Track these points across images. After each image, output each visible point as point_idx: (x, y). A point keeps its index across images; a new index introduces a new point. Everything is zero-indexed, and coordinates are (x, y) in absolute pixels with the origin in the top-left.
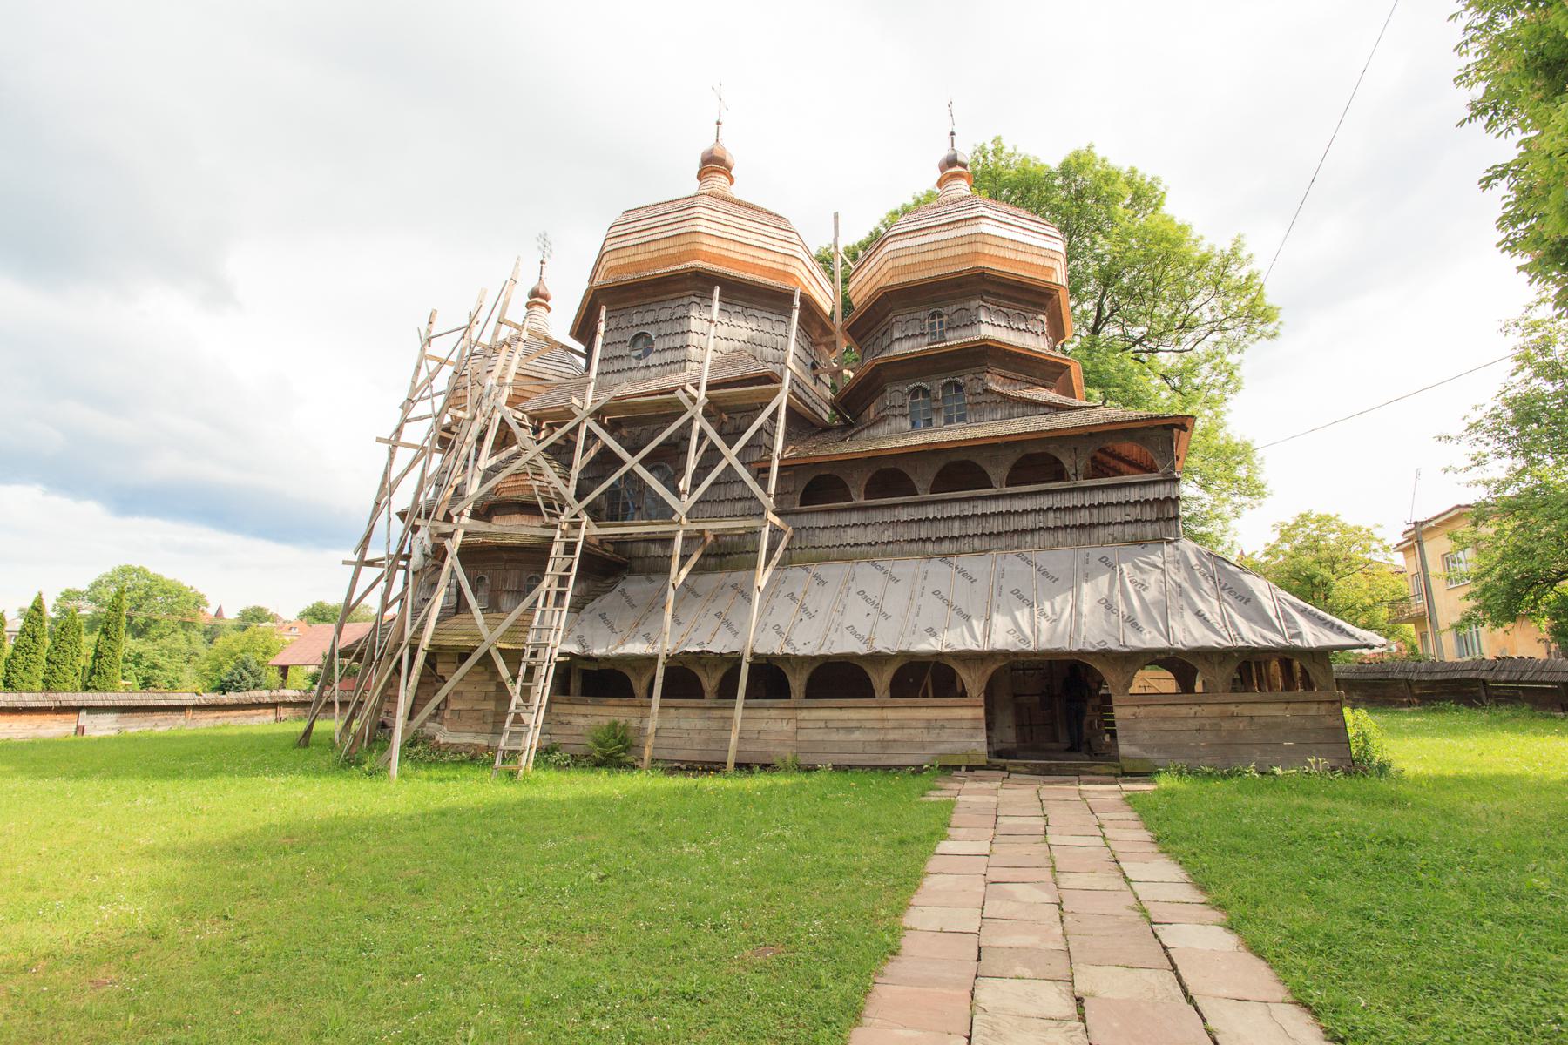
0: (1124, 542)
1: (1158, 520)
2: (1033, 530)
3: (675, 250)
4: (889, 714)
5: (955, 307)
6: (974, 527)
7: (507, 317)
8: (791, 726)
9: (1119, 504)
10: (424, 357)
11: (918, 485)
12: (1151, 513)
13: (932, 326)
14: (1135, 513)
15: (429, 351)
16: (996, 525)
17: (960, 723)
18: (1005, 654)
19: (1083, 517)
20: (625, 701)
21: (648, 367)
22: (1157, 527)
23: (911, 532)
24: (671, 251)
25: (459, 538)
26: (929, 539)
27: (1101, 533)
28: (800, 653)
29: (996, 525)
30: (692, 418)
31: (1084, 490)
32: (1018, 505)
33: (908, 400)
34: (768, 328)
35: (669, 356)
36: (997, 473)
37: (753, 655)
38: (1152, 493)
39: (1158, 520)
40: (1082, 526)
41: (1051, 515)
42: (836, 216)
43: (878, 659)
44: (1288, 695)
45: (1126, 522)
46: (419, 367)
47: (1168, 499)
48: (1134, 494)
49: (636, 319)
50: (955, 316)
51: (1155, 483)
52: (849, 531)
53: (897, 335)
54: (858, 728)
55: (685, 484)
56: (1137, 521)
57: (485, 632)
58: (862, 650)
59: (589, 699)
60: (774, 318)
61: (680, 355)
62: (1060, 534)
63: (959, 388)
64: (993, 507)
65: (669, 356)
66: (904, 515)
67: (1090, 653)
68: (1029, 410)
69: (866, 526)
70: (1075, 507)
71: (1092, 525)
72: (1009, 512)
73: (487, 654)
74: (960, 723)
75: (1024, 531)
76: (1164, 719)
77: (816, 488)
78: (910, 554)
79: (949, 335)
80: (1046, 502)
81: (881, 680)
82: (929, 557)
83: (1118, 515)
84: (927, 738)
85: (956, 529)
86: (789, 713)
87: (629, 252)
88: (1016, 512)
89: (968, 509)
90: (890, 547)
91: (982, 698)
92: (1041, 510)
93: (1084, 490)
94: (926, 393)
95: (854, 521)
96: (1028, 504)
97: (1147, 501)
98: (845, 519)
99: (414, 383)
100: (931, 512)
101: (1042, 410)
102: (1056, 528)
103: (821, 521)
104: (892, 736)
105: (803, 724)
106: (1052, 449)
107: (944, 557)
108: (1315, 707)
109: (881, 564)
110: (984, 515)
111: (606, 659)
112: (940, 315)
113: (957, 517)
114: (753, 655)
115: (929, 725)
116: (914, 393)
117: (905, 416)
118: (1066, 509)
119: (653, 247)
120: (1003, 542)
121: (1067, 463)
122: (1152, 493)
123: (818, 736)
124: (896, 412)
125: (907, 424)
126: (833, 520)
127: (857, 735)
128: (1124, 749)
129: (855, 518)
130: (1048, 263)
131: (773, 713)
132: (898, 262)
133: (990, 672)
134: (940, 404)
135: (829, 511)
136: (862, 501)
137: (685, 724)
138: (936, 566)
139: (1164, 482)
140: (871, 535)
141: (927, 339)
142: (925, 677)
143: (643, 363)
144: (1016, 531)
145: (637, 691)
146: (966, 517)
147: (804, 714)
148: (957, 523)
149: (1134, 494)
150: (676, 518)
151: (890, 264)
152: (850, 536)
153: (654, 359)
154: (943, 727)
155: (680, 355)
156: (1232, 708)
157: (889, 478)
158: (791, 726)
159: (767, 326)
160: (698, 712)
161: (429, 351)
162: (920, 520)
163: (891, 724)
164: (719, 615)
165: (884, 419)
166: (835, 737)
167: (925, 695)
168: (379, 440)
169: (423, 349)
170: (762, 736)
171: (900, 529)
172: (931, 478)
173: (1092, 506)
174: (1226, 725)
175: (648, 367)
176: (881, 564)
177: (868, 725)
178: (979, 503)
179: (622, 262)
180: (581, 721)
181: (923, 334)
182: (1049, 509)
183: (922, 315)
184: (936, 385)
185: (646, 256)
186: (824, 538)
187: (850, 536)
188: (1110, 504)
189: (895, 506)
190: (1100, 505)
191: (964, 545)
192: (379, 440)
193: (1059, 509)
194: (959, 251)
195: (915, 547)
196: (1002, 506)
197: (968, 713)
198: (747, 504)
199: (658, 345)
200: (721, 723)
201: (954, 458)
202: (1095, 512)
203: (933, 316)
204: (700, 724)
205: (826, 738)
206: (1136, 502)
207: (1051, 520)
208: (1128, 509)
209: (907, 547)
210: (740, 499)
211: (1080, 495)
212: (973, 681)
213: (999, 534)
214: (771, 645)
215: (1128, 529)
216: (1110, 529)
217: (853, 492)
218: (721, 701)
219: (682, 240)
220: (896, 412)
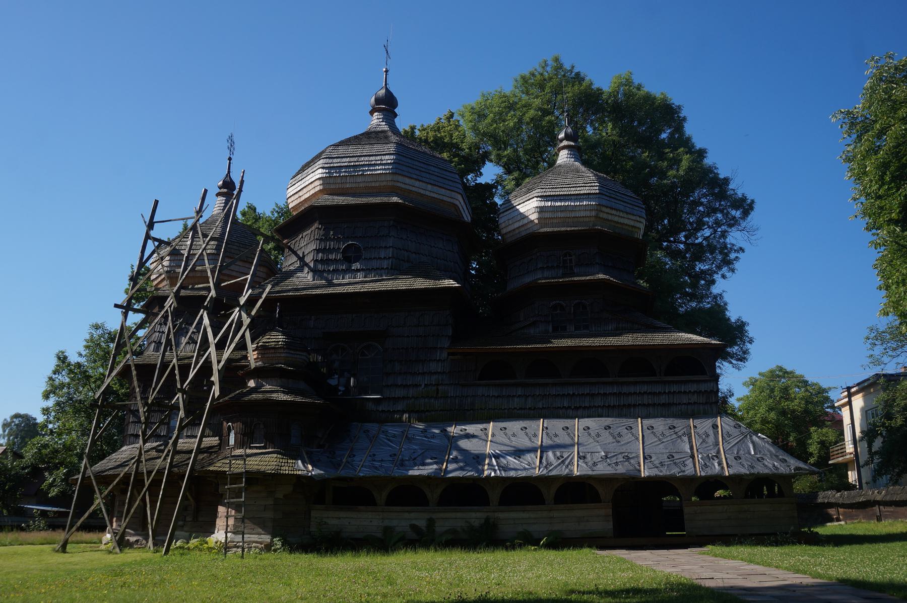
2: (635, 406)
9: (685, 392)
10: (148, 237)
14: (694, 398)
15: (153, 233)
19: (663, 399)
26: (569, 407)
38: (703, 387)
45: (689, 404)
47: (712, 391)
56: (695, 403)
64: (609, 390)
70: (660, 393)
72: (620, 393)
80: (645, 388)
96: (632, 389)
97: (700, 391)
102: (649, 405)
110: (605, 394)
112: (570, 256)
118: (654, 394)
122: (703, 387)
129: (520, 392)
130: (638, 225)
139: (710, 381)
149: (693, 387)
161: (153, 233)
162: (564, 395)
168: (116, 306)
188: (680, 392)
192: (116, 306)
193: (650, 393)
206: (695, 392)
207: (646, 400)
213: (614, 406)
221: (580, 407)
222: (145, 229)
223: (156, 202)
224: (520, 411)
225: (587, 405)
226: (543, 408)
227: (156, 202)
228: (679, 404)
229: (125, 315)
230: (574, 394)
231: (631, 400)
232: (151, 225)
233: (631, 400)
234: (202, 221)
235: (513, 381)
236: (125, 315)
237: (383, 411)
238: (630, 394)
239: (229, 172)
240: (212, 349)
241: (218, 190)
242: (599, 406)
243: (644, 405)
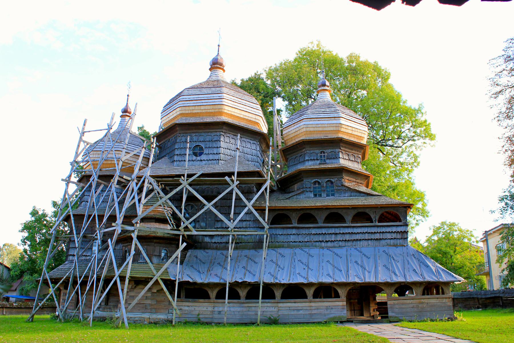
0: (390, 245)
1: (401, 238)
2: (360, 240)
3: (213, 111)
4: (313, 304)
5: (330, 151)
6: (339, 238)
8: (276, 309)
9: (389, 232)
10: (81, 140)
11: (319, 221)
12: (399, 236)
13: (321, 156)
14: (394, 236)
16: (347, 237)
17: (338, 306)
18: (355, 284)
19: (377, 236)
20: (207, 300)
21: (201, 160)
22: (401, 241)
23: (316, 238)
24: (211, 111)
25: (136, 233)
26: (323, 241)
27: (383, 242)
28: (282, 282)
29: (347, 237)
30: (232, 190)
31: (378, 226)
32: (356, 230)
33: (312, 186)
34: (249, 147)
35: (211, 157)
36: (349, 218)
37: (264, 283)
38: (400, 229)
39: (401, 238)
40: (377, 239)
41: (367, 235)
43: (310, 285)
44: (438, 296)
46: (79, 146)
47: (405, 231)
48: (394, 229)
49: (195, 139)
50: (330, 154)
51: (401, 226)
52: (291, 236)
53: (307, 158)
54: (301, 310)
55: (232, 216)
56: (395, 238)
57: (155, 272)
58: (305, 281)
59: (190, 300)
60: (252, 142)
61: (216, 157)
62: (370, 241)
63: (332, 183)
65: (211, 157)
66: (314, 231)
67: (381, 283)
68: (358, 194)
69: (298, 235)
70: (375, 233)
71: (380, 239)
72: (352, 233)
73: (157, 282)
75: (357, 240)
76: (403, 304)
77: (280, 218)
78: (316, 246)
79: (328, 161)
80: (365, 230)
81: (310, 292)
82: (323, 248)
83: (389, 236)
84: (326, 312)
85: (333, 238)
86: (275, 305)
87: (191, 108)
88: (355, 233)
89: (337, 231)
90: (308, 243)
91: (345, 298)
92: (363, 233)
93: (378, 226)
94: (319, 183)
97: (398, 232)
98: (290, 231)
99: (77, 153)
100: (324, 231)
101: (362, 195)
102: (368, 239)
103: (280, 232)
104: (314, 312)
105: (280, 309)
106: (367, 211)
107: (328, 248)
108: (445, 299)
109: (305, 250)
110: (343, 233)
111: (202, 284)
112: (324, 153)
113: (333, 233)
114: (264, 283)
115: (327, 308)
116: (315, 183)
117: (311, 192)
118: (372, 233)
119: (202, 108)
120: (350, 243)
121: (372, 216)
122: (400, 229)
123: (286, 313)
124: (308, 190)
125: (312, 195)
126: (285, 232)
127: (301, 312)
128: (390, 314)
129: (294, 231)
130: (363, 136)
131: (269, 305)
132: (308, 129)
133: (348, 289)
134: (324, 189)
135: (283, 228)
136: (296, 225)
137: (232, 309)
138: (326, 252)
139: (404, 225)
140: (300, 238)
141: (318, 162)
142: (325, 291)
143: (199, 158)
144: (354, 240)
145: (211, 296)
146: (336, 234)
148: (333, 236)
149: (394, 229)
150: (229, 229)
151: (304, 130)
152: (292, 238)
153: (203, 157)
154: (332, 308)
155: (216, 157)
156: (422, 300)
158: (276, 309)
159: (249, 145)
160: (238, 305)
161: (84, 138)
162: (320, 234)
163: (313, 308)
164: (244, 267)
165: (303, 192)
166: (292, 313)
167: (321, 298)
168: (63, 180)
169: (81, 138)
170: (265, 313)
171: (312, 237)
172: (324, 218)
173: (380, 232)
174: (420, 306)
175: (201, 160)
176: (305, 250)
177: (305, 308)
178: (342, 229)
179: (187, 112)
180: (187, 308)
181: (317, 159)
182: (366, 232)
183: (317, 151)
184: (323, 180)
185: (199, 111)
186: (281, 239)
187: (292, 238)
188: (387, 232)
189: (310, 228)
190: (383, 232)
191: (335, 244)
192: (63, 180)
193: (369, 233)
194: (332, 129)
195: (317, 244)
196: (350, 230)
197: (341, 304)
198: (248, 223)
199: (206, 151)
200: (248, 309)
201: (333, 211)
202: (381, 234)
203: (321, 153)
204: (239, 309)
205: (289, 313)
206: (395, 232)
207: (367, 236)
208: (392, 234)
209: (314, 243)
210: (245, 221)
211: (377, 228)
212: (343, 292)
213: (348, 240)
214: (269, 280)
215: (392, 241)
216: (386, 241)
217: (293, 221)
218: (248, 301)
219: (216, 107)
220: (308, 190)
222: (80, 135)
223: (85, 121)
224: (294, 243)
227: (85, 121)
229: (67, 185)
231: (358, 237)
232: (83, 133)
233: (358, 237)
234: (112, 131)
235: (290, 226)
236: (67, 185)
237: (215, 243)
238: (358, 233)
239: (127, 104)
240: (116, 205)
241: (121, 114)
242: (340, 240)
243: (366, 240)
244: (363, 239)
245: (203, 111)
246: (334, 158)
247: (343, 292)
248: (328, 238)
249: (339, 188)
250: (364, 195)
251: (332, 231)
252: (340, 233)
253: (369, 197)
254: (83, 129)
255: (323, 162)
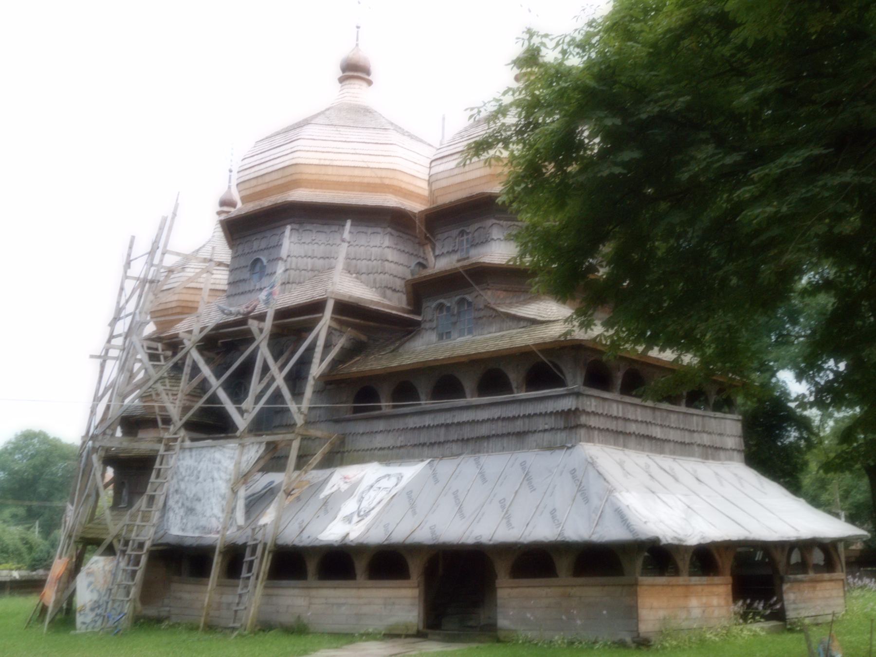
6: (454, 434)
7: (168, 248)
14: (550, 422)
15: (128, 274)
16: (467, 432)
17: (402, 602)
19: (519, 426)
27: (531, 439)
29: (467, 432)
41: (500, 423)
42: (444, 119)
45: (545, 431)
46: (122, 289)
50: (476, 234)
56: (552, 429)
63: (470, 304)
66: (412, 422)
74: (402, 602)
80: (496, 412)
85: (442, 435)
88: (478, 421)
89: (447, 418)
92: (493, 419)
95: (381, 428)
99: (118, 303)
100: (427, 420)
101: (522, 324)
103: (361, 427)
110: (459, 424)
113: (442, 424)
118: (508, 419)
129: (381, 425)
144: (478, 438)
146: (447, 426)
147: (314, 592)
148: (443, 431)
154: (394, 604)
157: (404, 386)
161: (130, 273)
168: (92, 357)
169: (126, 272)
173: (524, 416)
178: (456, 413)
182: (499, 418)
183: (455, 232)
188: (535, 414)
190: (529, 415)
192: (92, 357)
193: (504, 419)
202: (527, 421)
203: (462, 233)
206: (551, 413)
207: (500, 428)
212: (416, 567)
213: (468, 440)
221: (435, 443)
223: (133, 239)
225: (442, 440)
226: (401, 447)
227: (133, 239)
228: (535, 431)
230: (429, 426)
233: (484, 430)
238: (483, 421)
242: (453, 441)
244: (493, 435)
245: (271, 185)
246: (482, 243)
247: (416, 567)
248: (433, 436)
249: (482, 314)
250: (525, 324)
251: (441, 419)
252: (453, 424)
253: (533, 327)
254: (129, 255)
255: (465, 256)
